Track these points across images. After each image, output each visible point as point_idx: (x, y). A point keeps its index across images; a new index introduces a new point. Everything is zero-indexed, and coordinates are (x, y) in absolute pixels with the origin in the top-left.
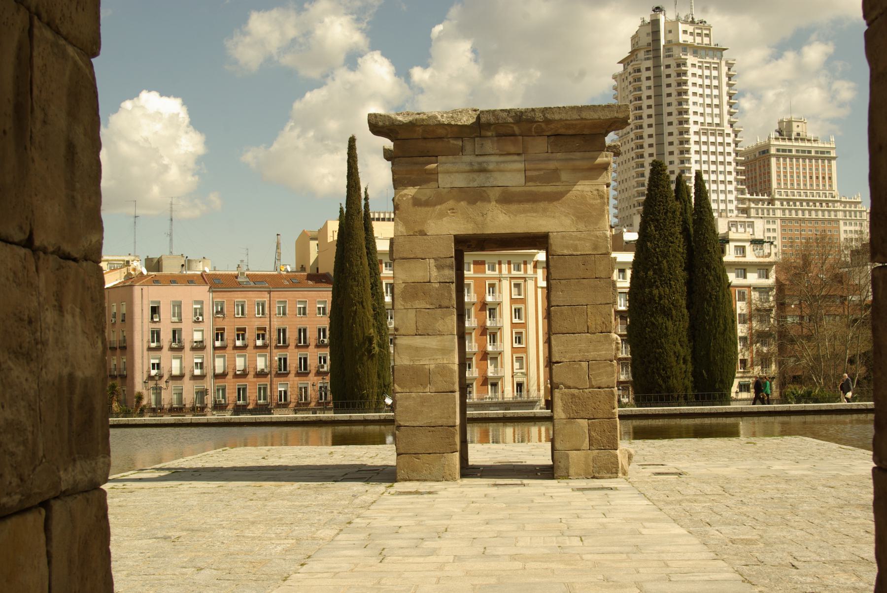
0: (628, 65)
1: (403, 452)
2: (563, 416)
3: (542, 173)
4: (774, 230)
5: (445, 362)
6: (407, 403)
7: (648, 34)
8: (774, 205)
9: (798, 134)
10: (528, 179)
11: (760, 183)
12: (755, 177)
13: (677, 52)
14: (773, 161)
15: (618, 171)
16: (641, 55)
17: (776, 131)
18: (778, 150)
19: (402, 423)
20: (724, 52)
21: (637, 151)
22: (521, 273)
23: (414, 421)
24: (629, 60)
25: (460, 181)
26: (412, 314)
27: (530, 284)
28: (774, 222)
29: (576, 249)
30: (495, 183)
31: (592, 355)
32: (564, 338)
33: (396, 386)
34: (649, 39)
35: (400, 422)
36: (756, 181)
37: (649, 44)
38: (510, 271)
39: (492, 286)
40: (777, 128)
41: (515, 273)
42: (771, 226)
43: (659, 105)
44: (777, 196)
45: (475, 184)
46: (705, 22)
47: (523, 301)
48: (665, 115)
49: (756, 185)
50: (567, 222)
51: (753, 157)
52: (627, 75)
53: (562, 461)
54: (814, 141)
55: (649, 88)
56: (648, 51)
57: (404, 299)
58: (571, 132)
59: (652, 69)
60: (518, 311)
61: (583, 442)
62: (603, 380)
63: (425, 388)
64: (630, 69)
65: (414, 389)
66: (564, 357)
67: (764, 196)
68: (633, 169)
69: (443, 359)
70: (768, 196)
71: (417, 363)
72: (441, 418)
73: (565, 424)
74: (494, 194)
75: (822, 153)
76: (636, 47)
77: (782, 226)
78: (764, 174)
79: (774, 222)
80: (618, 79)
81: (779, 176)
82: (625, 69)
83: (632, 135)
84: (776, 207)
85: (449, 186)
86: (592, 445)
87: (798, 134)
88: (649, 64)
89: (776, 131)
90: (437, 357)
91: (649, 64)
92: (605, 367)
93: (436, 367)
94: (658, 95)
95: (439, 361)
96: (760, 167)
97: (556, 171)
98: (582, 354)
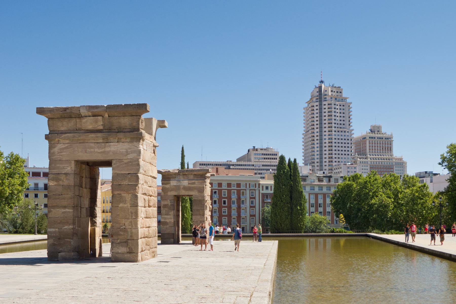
0: (309, 104)
4: (367, 169)
7: (317, 92)
10: (189, 184)
12: (361, 148)
13: (328, 98)
15: (305, 145)
17: (370, 130)
18: (370, 138)
20: (347, 99)
21: (312, 138)
22: (254, 188)
24: (310, 102)
25: (175, 184)
27: (257, 192)
28: (367, 166)
29: (198, 198)
30: (182, 184)
32: (195, 216)
36: (361, 149)
37: (318, 96)
38: (250, 187)
39: (243, 193)
40: (370, 129)
41: (251, 188)
42: (366, 168)
43: (321, 120)
45: (178, 185)
46: (340, 87)
47: (254, 198)
48: (323, 124)
49: (361, 151)
50: (197, 192)
51: (360, 140)
52: (309, 108)
54: (385, 134)
55: (317, 113)
57: (163, 207)
58: (198, 174)
59: (318, 106)
60: (252, 202)
64: (310, 106)
68: (310, 145)
70: (365, 156)
74: (182, 187)
75: (388, 139)
77: (370, 168)
78: (364, 147)
79: (367, 166)
80: (305, 109)
82: (308, 105)
83: (310, 132)
84: (368, 160)
88: (318, 104)
89: (370, 130)
91: (318, 104)
94: (321, 116)
96: (362, 144)
97: (194, 182)
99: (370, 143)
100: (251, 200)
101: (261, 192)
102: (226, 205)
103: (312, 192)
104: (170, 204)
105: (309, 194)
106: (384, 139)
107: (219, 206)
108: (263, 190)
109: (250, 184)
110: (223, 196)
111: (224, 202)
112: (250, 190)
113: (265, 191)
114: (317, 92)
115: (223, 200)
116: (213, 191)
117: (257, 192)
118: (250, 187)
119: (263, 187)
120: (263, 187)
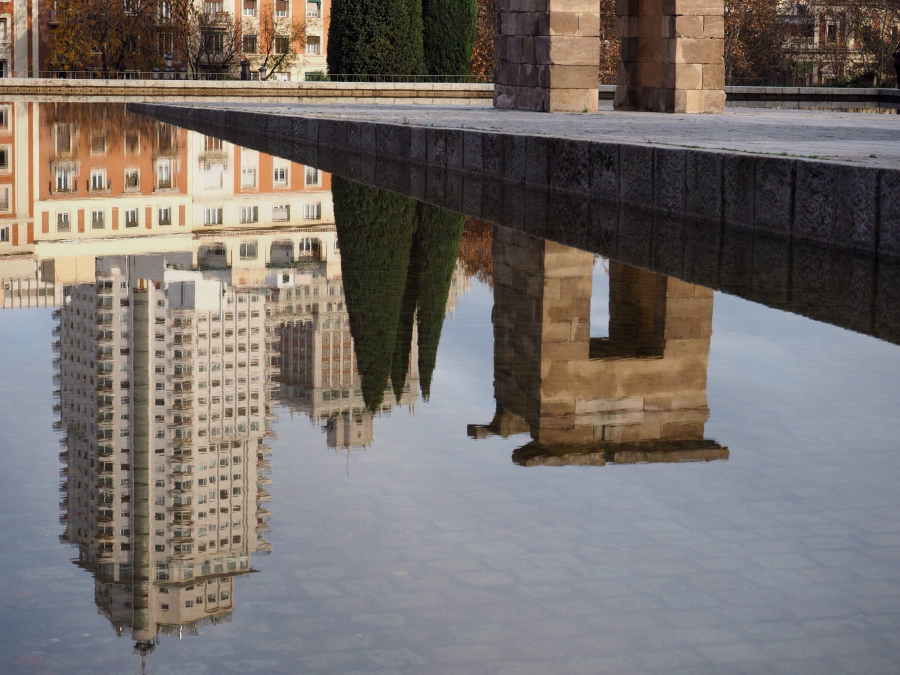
1: (555, 87)
2: (683, 61)
5: (592, 10)
6: (560, 45)
19: (556, 62)
23: (565, 60)
31: (707, 10)
33: (551, 29)
35: (554, 61)
53: (681, 98)
61: (698, 82)
62: (715, 32)
63: (574, 33)
65: (565, 34)
66: (685, 11)
69: (590, 8)
71: (569, 11)
72: (587, 59)
73: (685, 67)
86: (705, 86)
90: (585, 6)
92: (717, 20)
93: (584, 15)
95: (586, 10)
98: (699, 9)
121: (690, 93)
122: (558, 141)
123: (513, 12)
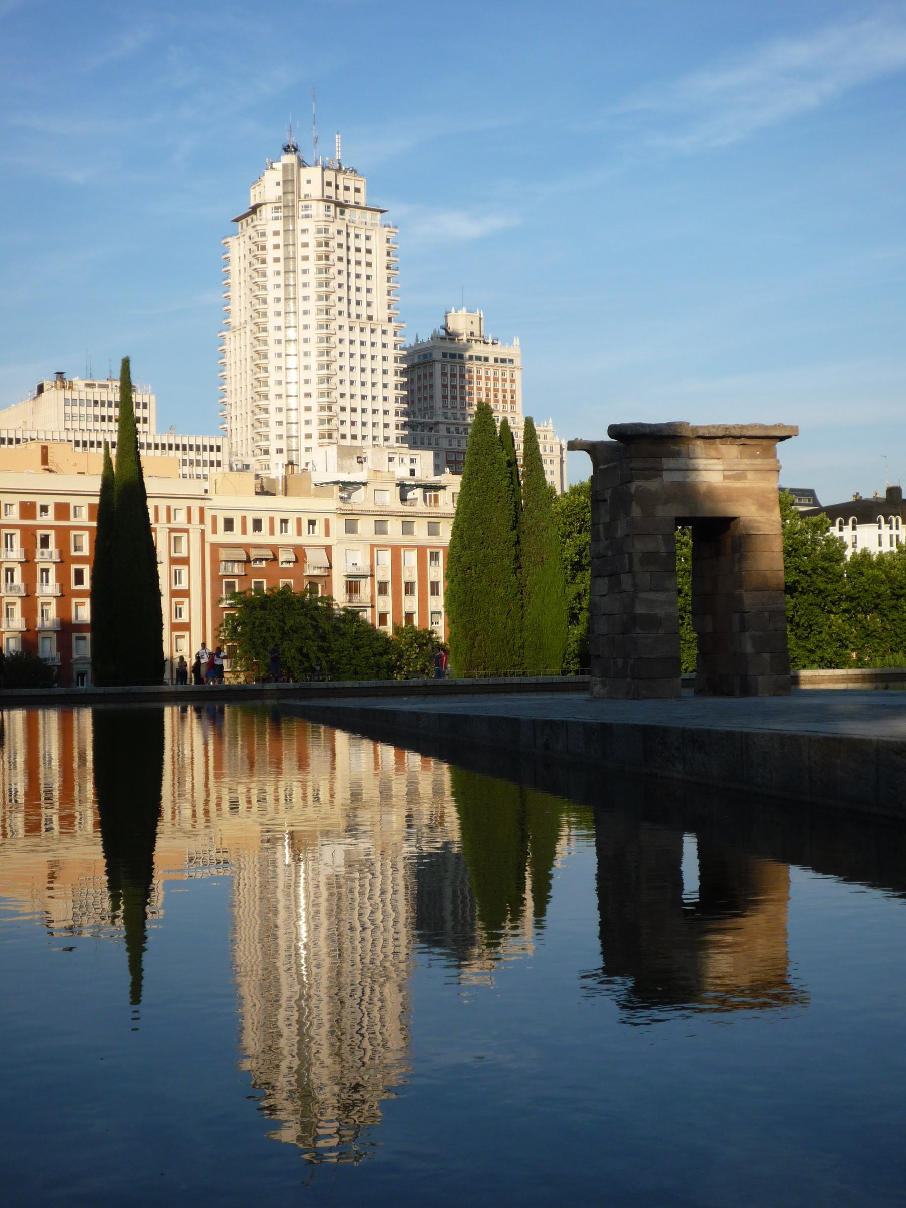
3: (735, 472)
7: (278, 184)
8: (438, 431)
9: (472, 334)
10: (726, 477)
11: (420, 399)
14: (438, 368)
16: (266, 212)
18: (445, 355)
26: (648, 575)
34: (280, 191)
38: (169, 521)
44: (441, 419)
56: (277, 208)
67: (424, 417)
76: (258, 201)
81: (444, 391)
85: (671, 480)
87: (472, 334)
91: (279, 225)
96: (419, 378)
99: (444, 375)
100: (174, 567)
101: (210, 538)
102: (87, 585)
103: (381, 539)
104: (663, 549)
105: (372, 547)
106: (491, 361)
107: (62, 590)
108: (215, 531)
109: (168, 508)
110: (73, 553)
111: (79, 574)
112: (171, 530)
113: (222, 537)
114: (278, 184)
115: (74, 567)
116: (39, 533)
117: (195, 537)
118: (169, 521)
119: (214, 519)
120: (214, 519)
121: (760, 679)
122: (653, 727)
123: (605, 614)
